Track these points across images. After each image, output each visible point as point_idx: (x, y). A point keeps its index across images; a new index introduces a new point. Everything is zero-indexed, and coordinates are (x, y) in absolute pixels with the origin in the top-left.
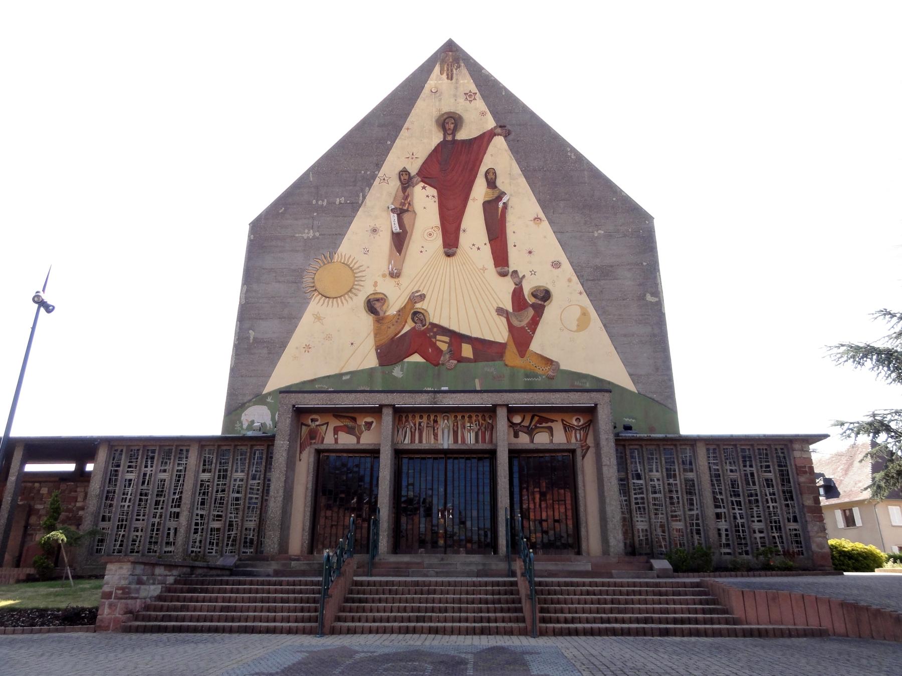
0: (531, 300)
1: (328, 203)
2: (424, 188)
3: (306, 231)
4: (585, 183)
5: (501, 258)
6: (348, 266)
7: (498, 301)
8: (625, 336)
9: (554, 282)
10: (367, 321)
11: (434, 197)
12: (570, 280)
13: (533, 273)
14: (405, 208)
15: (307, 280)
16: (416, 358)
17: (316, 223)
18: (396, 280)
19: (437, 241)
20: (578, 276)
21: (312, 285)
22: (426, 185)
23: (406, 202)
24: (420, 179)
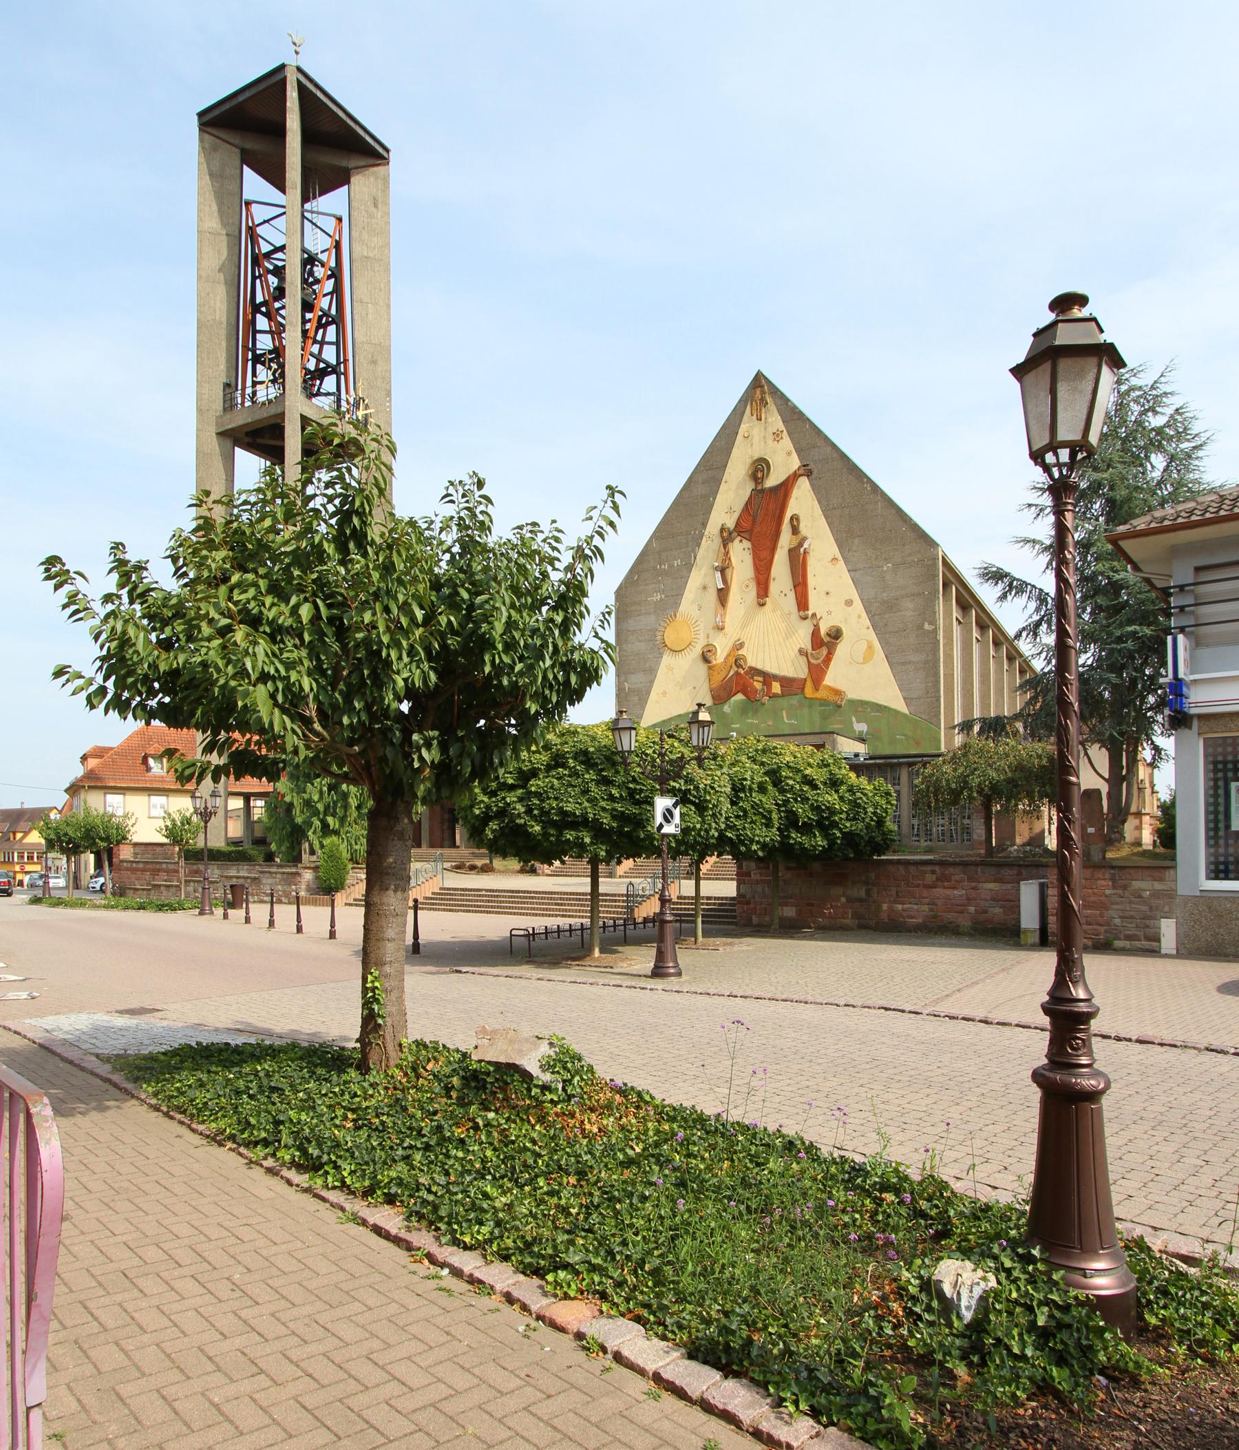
0: (826, 639)
5: (802, 603)
8: (903, 664)
10: (703, 668)
12: (859, 617)
13: (829, 613)
19: (752, 592)
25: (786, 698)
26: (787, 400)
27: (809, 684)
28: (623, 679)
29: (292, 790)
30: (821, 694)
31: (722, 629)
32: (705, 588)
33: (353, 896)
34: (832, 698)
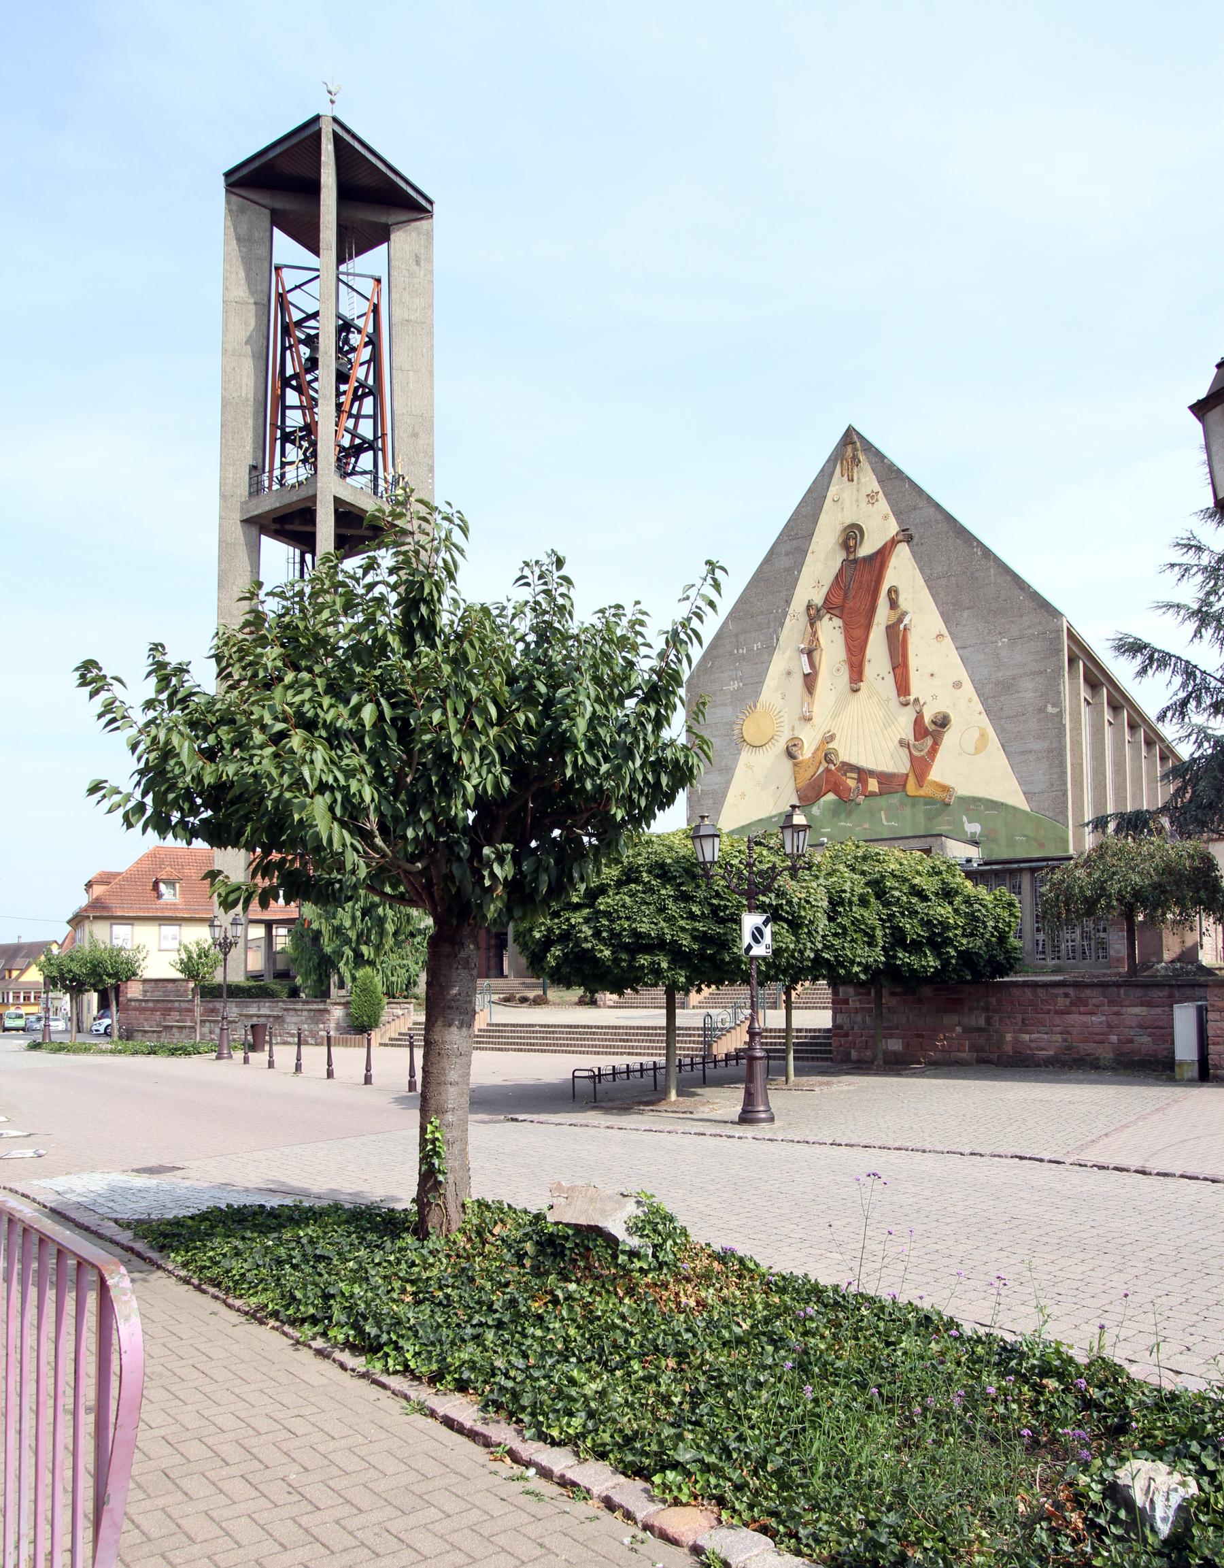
0: (931, 728)
5: (903, 687)
8: (1022, 753)
9: (954, 705)
10: (787, 764)
12: (970, 701)
13: (934, 697)
26: (883, 457)
27: (911, 782)
29: (320, 916)
30: (926, 791)
31: (810, 719)
32: (789, 673)
33: (388, 1035)
34: (939, 795)
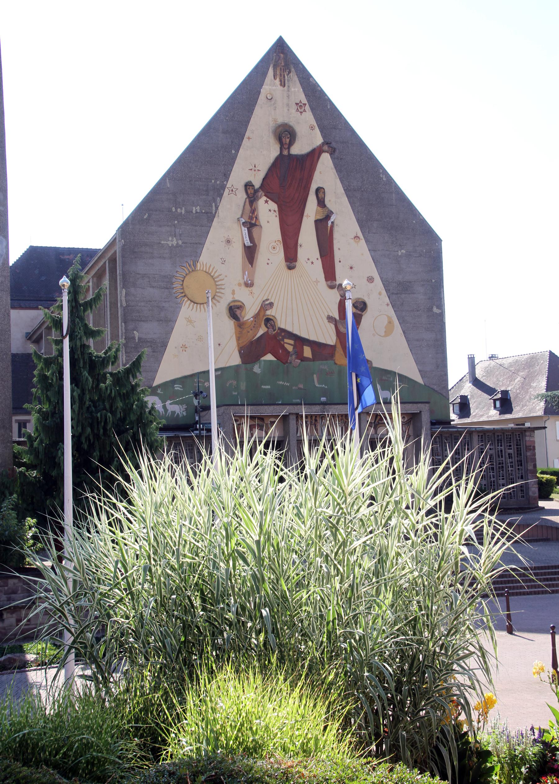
1: (186, 211)
2: (266, 202)
3: (170, 239)
4: (392, 205)
6: (210, 274)
7: (328, 310)
8: (417, 340)
9: (369, 295)
10: (229, 325)
11: (275, 211)
12: (380, 294)
14: (253, 222)
15: (177, 285)
16: (269, 357)
17: (177, 230)
18: (250, 289)
20: (386, 290)
21: (182, 291)
22: (268, 200)
23: (254, 216)
24: (263, 194)
25: (317, 363)
28: (131, 326)
31: (252, 285)
32: (228, 241)
